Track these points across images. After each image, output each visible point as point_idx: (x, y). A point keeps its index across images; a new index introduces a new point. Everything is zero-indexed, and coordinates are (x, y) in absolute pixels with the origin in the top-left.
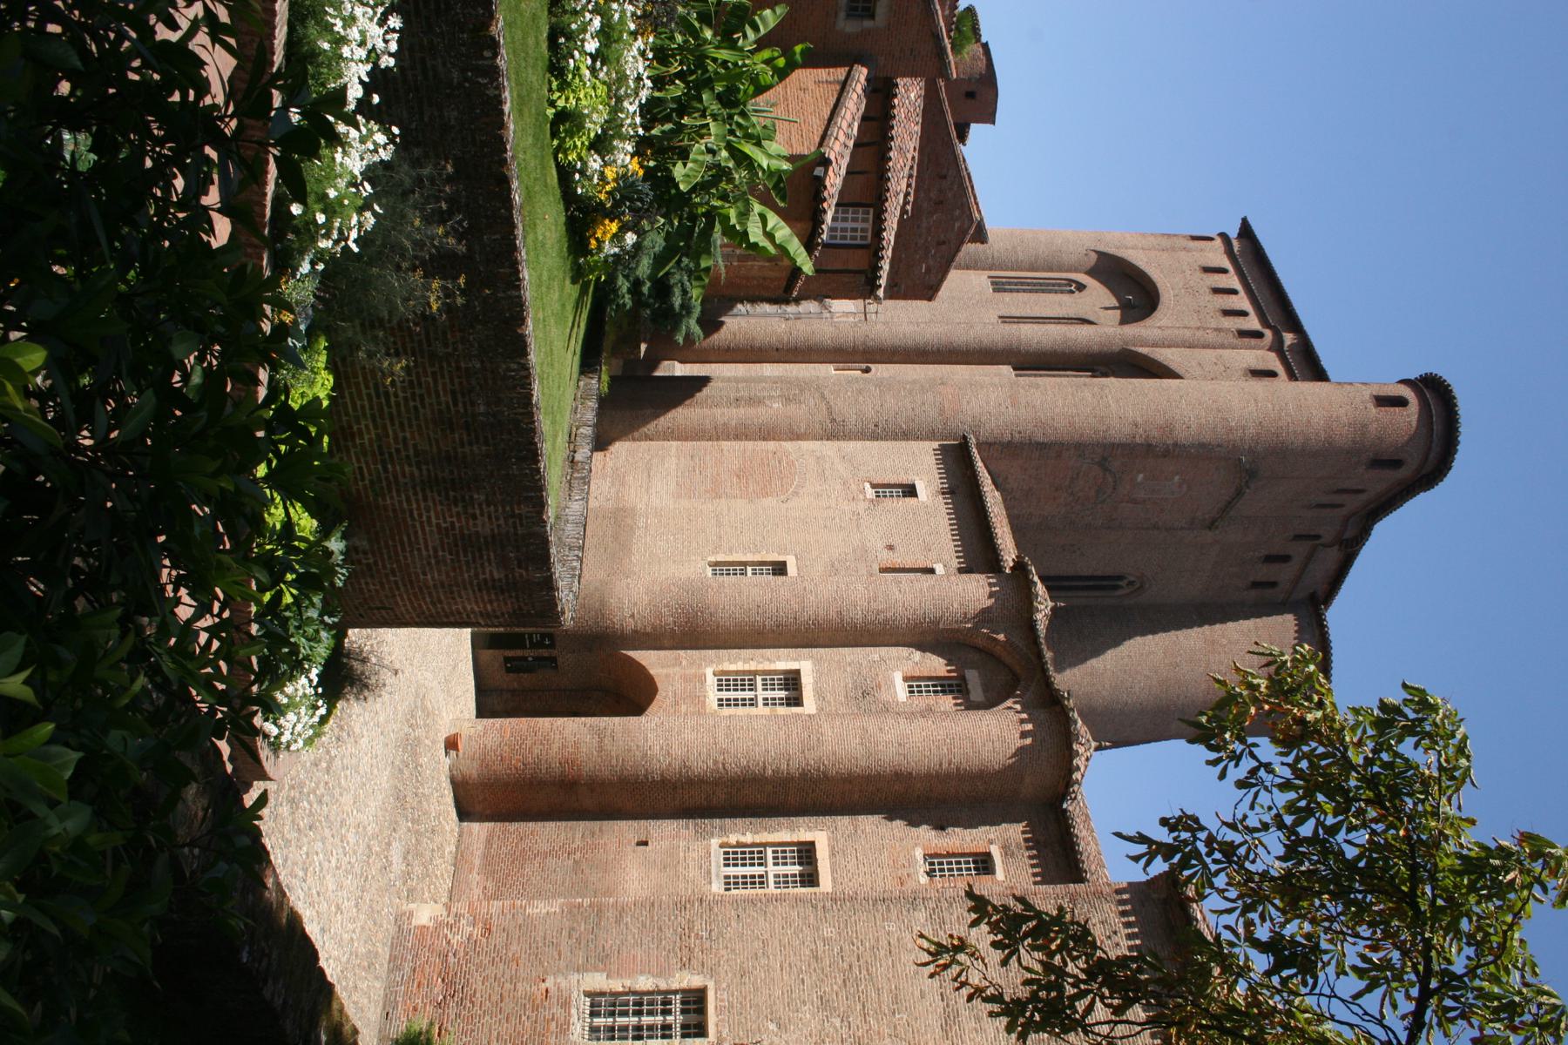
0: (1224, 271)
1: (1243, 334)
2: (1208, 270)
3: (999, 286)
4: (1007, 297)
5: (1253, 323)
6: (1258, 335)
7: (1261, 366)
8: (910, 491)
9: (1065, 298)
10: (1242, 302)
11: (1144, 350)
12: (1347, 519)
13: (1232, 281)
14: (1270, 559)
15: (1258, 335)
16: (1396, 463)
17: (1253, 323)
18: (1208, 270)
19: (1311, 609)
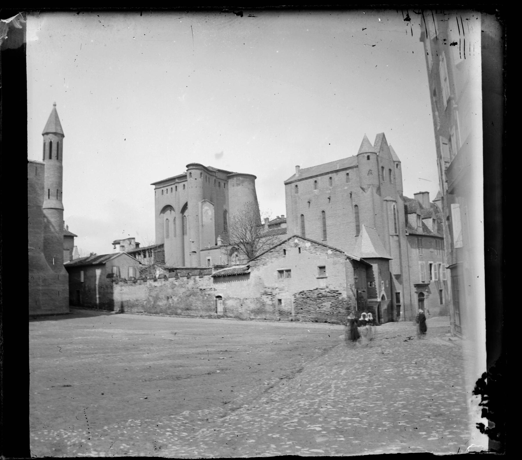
1: (176, 190)
2: (163, 194)
3: (168, 236)
4: (170, 235)
6: (176, 187)
8: (209, 260)
9: (170, 223)
10: (169, 188)
11: (180, 210)
12: (211, 175)
13: (165, 189)
14: (219, 186)
15: (176, 187)
16: (201, 173)
17: (174, 187)
18: (163, 194)
19: (229, 175)
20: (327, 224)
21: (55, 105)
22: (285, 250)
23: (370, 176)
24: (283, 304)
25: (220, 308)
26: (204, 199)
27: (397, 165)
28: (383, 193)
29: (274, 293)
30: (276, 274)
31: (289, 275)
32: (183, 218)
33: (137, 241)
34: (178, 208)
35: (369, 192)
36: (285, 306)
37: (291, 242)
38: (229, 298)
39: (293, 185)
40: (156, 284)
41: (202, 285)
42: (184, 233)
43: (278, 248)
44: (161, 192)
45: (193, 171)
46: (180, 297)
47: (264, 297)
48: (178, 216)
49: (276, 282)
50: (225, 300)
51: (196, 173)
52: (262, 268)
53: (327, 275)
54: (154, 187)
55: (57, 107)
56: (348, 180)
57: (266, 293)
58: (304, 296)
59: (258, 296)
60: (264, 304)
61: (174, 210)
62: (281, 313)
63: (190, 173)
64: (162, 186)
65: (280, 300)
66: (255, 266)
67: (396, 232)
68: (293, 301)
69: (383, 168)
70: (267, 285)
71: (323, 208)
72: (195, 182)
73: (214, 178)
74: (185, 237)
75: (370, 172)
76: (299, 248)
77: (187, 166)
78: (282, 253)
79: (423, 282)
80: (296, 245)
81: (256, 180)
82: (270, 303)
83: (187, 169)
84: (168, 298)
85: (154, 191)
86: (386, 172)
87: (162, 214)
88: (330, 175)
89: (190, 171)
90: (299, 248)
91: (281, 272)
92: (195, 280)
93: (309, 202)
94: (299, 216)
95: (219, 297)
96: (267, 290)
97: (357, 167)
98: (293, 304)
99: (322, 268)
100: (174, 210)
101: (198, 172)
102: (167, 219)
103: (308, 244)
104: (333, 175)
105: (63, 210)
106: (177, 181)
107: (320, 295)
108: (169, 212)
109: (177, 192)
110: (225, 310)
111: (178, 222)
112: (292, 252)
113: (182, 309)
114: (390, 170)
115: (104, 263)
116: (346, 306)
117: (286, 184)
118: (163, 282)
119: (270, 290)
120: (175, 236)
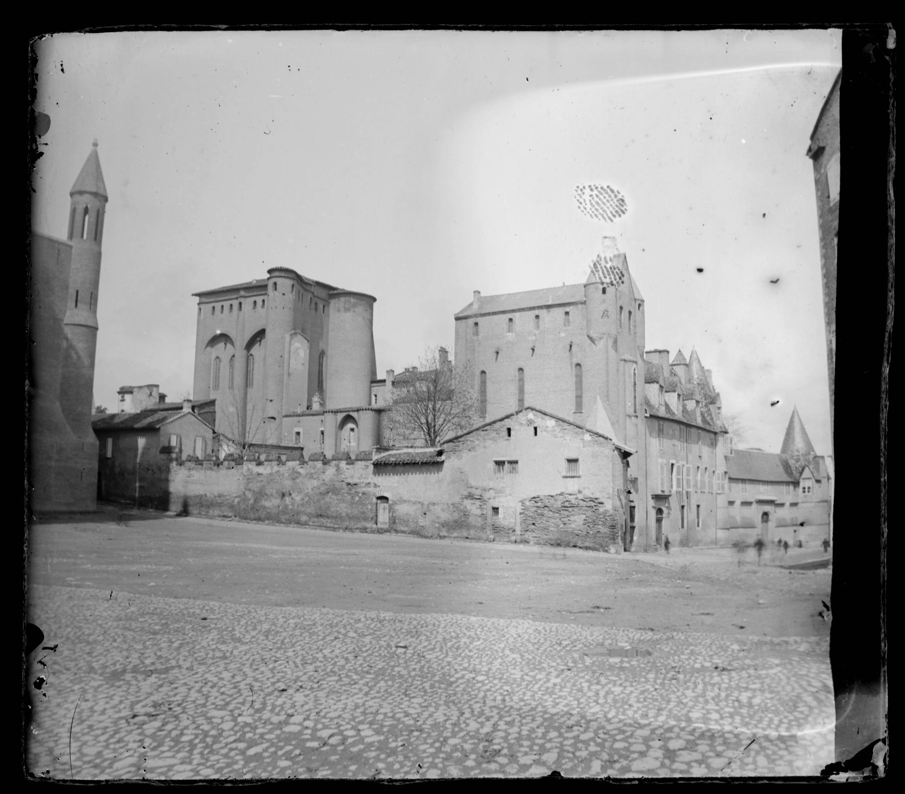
0: (214, 308)
3: (216, 387)
5: (235, 303)
6: (240, 304)
7: (252, 305)
8: (298, 433)
9: (222, 365)
10: (226, 304)
11: (245, 345)
12: (306, 290)
13: (218, 306)
14: (316, 309)
15: (240, 304)
16: (293, 285)
17: (235, 303)
19: (332, 293)
20: (526, 390)
21: (95, 145)
22: (509, 430)
23: (605, 319)
24: (501, 515)
25: (384, 517)
26: (294, 329)
27: (639, 305)
28: (620, 348)
29: (486, 496)
30: (492, 465)
31: (514, 469)
32: (249, 358)
33: (162, 390)
34: (241, 340)
35: (601, 344)
36: (504, 518)
37: (522, 417)
38: (402, 501)
39: (471, 322)
40: (260, 469)
41: (352, 477)
42: (248, 382)
43: (498, 425)
44: (211, 309)
45: (280, 281)
46: (307, 495)
47: (468, 503)
48: (241, 353)
49: (490, 479)
50: (395, 503)
51: (285, 284)
52: (466, 456)
53: (581, 473)
54: (197, 298)
55: (99, 149)
56: (567, 323)
57: (470, 496)
58: (539, 504)
59: (457, 499)
60: (466, 514)
61: (232, 344)
62: (496, 529)
63: (275, 284)
64: (212, 300)
65: (496, 510)
66: (454, 451)
67: (635, 412)
68: (519, 510)
69: (621, 308)
70: (473, 482)
71: (521, 364)
72: (282, 298)
73: (310, 296)
74: (249, 390)
75: (605, 314)
76: (535, 429)
77: (270, 272)
78: (506, 433)
79: (663, 491)
80: (530, 422)
81: (375, 304)
82: (478, 512)
83: (268, 276)
84: (283, 495)
85: (197, 306)
86: (625, 313)
87: (209, 348)
88: (537, 312)
89: (274, 280)
90: (535, 429)
91: (500, 464)
92: (338, 468)
93: (497, 353)
94: (478, 373)
95: (384, 499)
96: (473, 491)
97: (584, 303)
98: (518, 516)
99: (572, 461)
100: (232, 344)
101: (289, 283)
102: (217, 357)
103: (551, 423)
104: (543, 313)
105: (97, 329)
106: (242, 293)
107: (567, 504)
108: (222, 345)
109: (241, 314)
110: (393, 520)
111: (239, 363)
112: (522, 432)
113: (310, 515)
114: (630, 313)
115: (158, 427)
116: (609, 523)
117: (458, 319)
118: (276, 468)
119: (478, 492)
120: (231, 387)
